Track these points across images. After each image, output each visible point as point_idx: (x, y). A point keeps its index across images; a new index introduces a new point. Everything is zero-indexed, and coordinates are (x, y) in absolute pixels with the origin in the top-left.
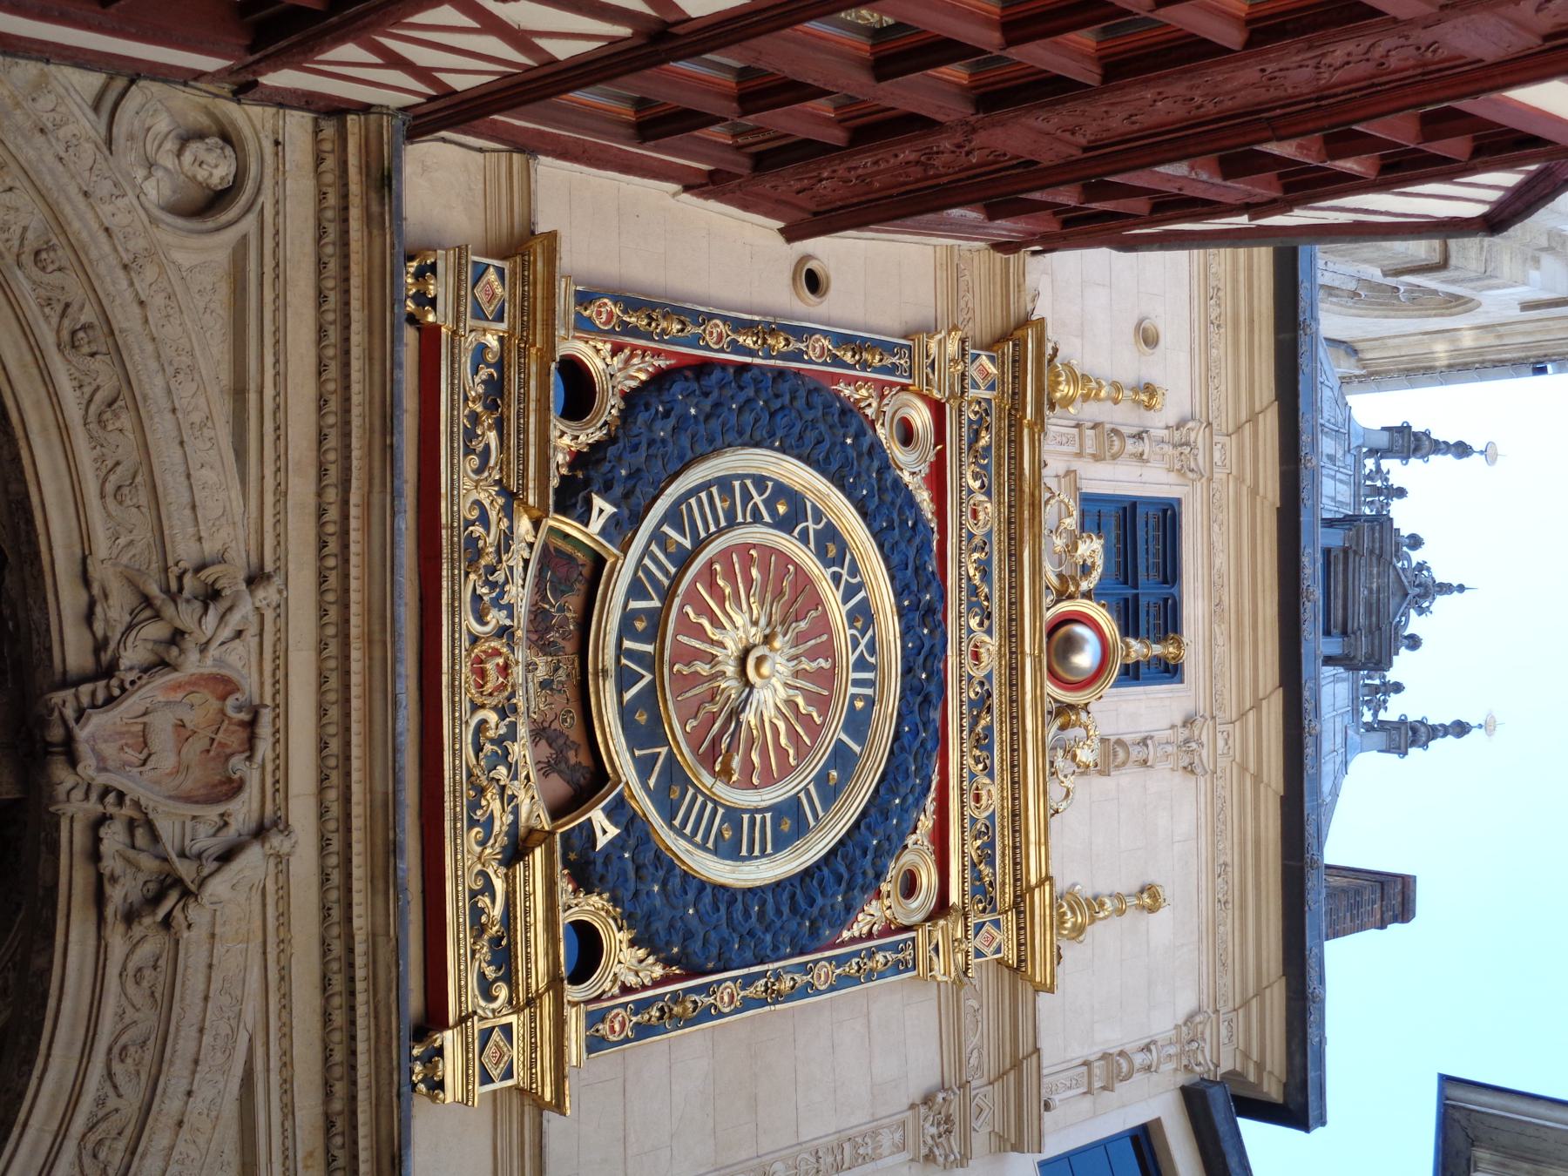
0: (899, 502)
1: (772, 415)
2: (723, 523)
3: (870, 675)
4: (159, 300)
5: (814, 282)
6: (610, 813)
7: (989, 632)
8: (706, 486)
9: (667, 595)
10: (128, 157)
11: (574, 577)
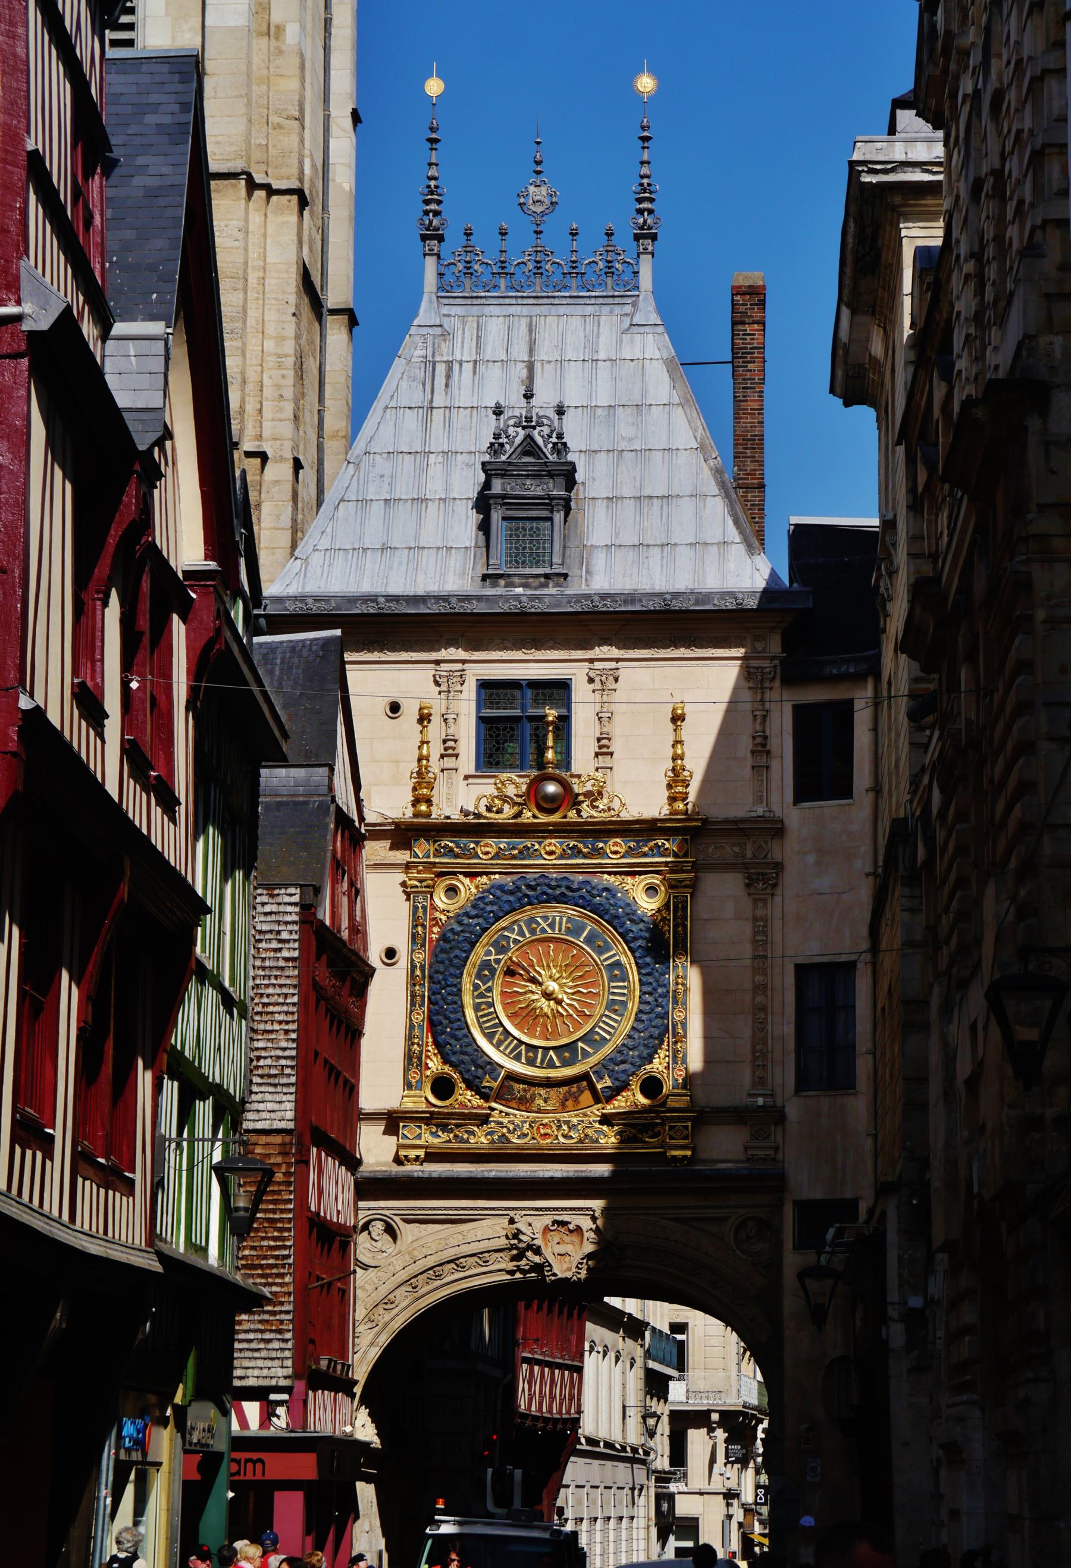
0: (482, 905)
1: (448, 986)
2: (492, 1010)
4: (424, 1250)
5: (391, 953)
6: (601, 1078)
9: (521, 1042)
10: (380, 1259)
11: (512, 1090)
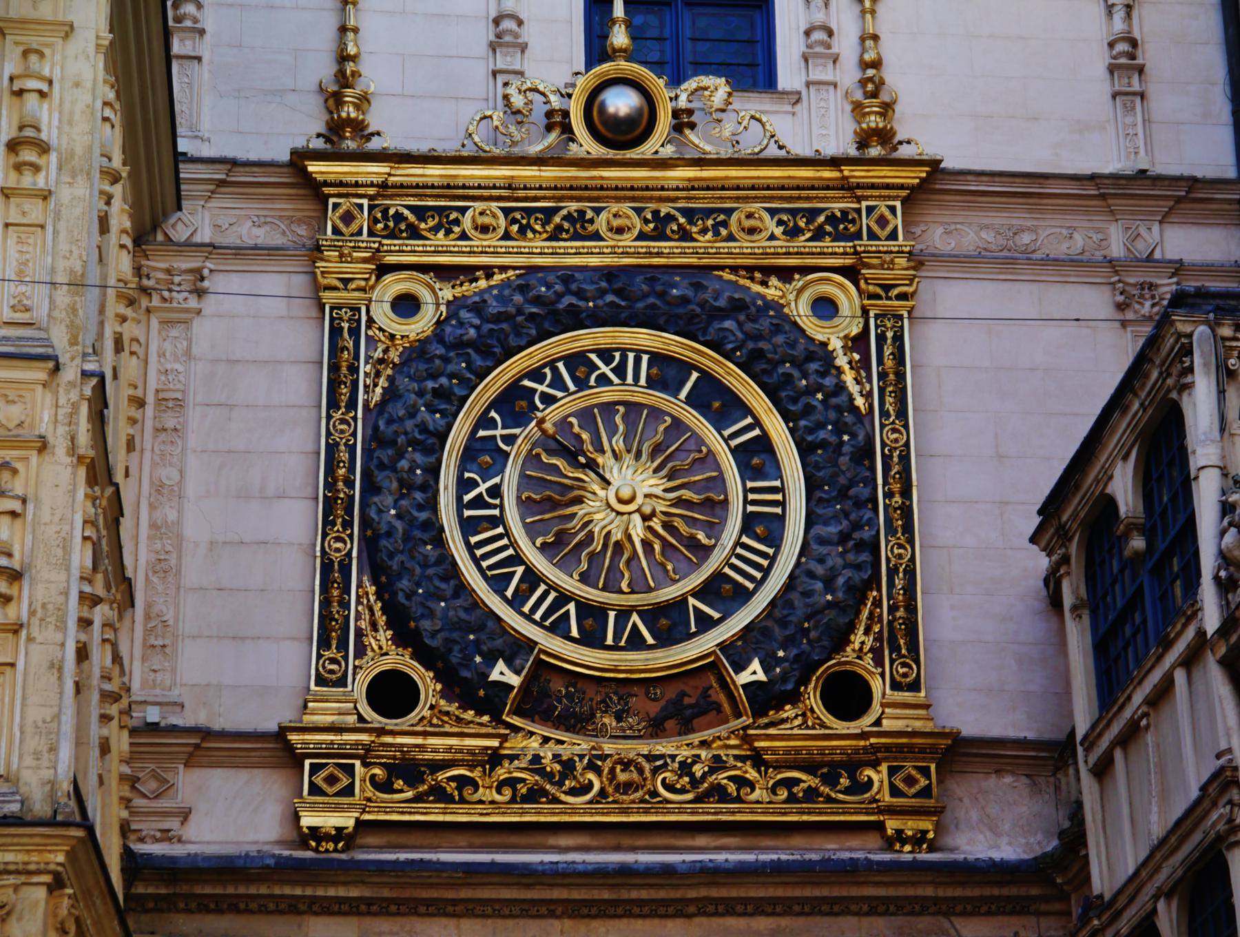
2: (500, 530)
3: (631, 356)
6: (739, 668)
7: (598, 211)
8: (470, 548)
9: (564, 598)
